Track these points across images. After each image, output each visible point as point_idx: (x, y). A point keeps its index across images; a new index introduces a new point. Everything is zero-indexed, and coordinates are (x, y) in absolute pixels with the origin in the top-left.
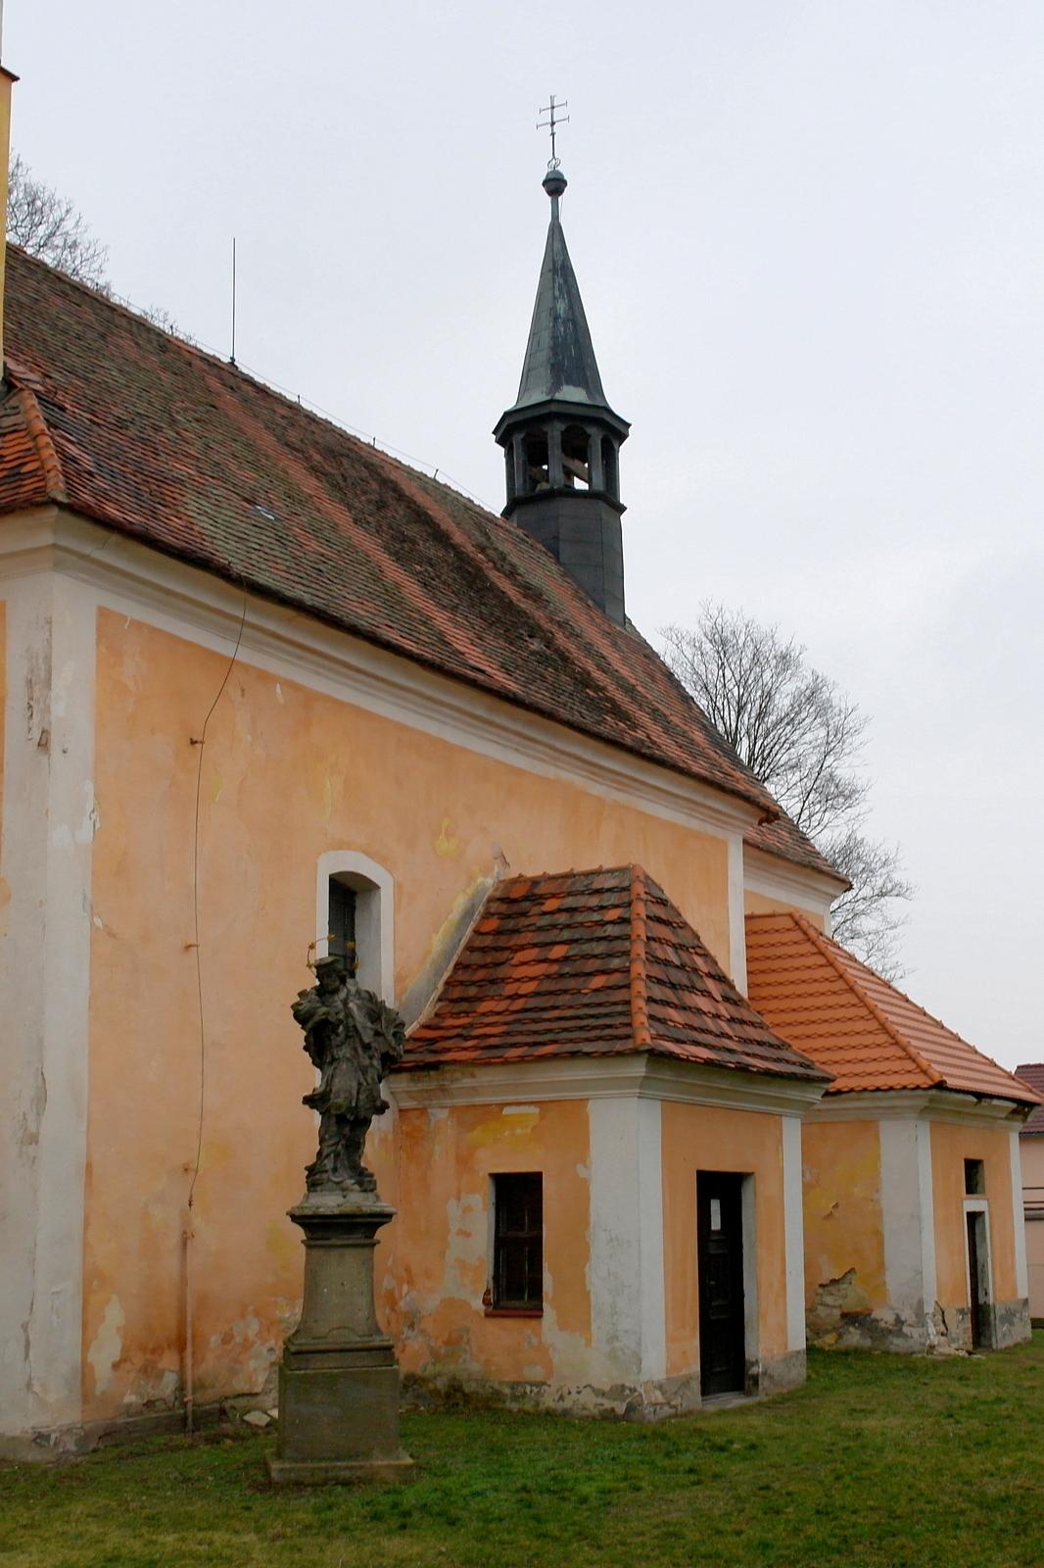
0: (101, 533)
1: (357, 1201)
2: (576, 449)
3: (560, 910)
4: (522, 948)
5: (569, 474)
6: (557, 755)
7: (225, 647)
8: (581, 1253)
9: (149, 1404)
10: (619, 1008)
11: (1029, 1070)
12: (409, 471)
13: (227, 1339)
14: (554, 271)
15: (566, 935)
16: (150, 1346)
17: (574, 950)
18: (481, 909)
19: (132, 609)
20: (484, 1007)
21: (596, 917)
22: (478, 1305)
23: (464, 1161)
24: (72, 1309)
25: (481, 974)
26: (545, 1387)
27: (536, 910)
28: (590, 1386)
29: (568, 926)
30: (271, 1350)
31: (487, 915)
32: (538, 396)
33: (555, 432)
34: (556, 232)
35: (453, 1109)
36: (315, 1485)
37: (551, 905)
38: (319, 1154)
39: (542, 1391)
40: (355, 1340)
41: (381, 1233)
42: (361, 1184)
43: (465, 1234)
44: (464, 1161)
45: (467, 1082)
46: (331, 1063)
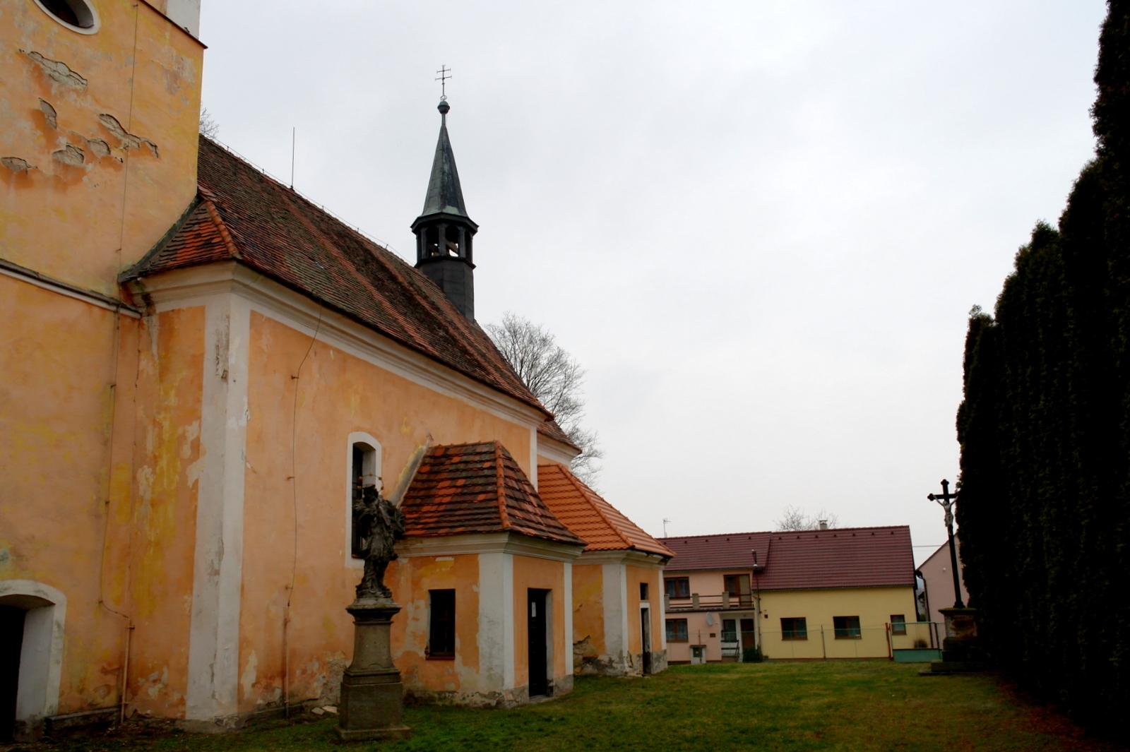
0: (255, 274)
1: (383, 602)
2: (453, 236)
3: (460, 462)
4: (442, 480)
5: (448, 248)
6: (455, 387)
7: (310, 332)
8: (475, 628)
9: (269, 704)
10: (493, 510)
11: (883, 530)
12: (375, 245)
13: (304, 672)
14: (443, 150)
15: (464, 474)
16: (269, 675)
17: (469, 482)
18: (420, 461)
19: (267, 313)
20: (425, 509)
21: (479, 466)
22: (422, 654)
23: (416, 584)
24: (234, 658)
25: (422, 493)
26: (456, 694)
27: (448, 462)
28: (478, 692)
29: (464, 470)
30: (324, 677)
31: (424, 464)
32: (434, 211)
33: (442, 228)
34: (444, 131)
35: (411, 558)
36: (363, 741)
37: (456, 459)
38: (364, 580)
40: (381, 669)
41: (394, 617)
42: (384, 594)
43: (416, 619)
44: (416, 584)
45: (419, 545)
46: (370, 536)
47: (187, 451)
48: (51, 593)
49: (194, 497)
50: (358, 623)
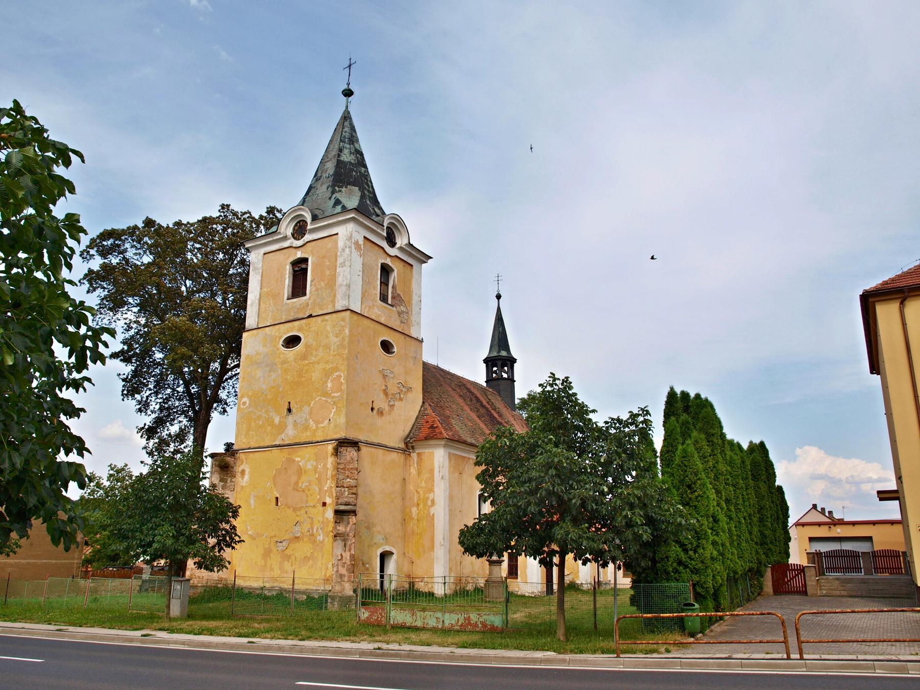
19: (453, 451)
32: (495, 354)
33: (499, 363)
34: (499, 309)
47: (429, 503)
48: (394, 551)
49: (433, 519)
50: (490, 565)
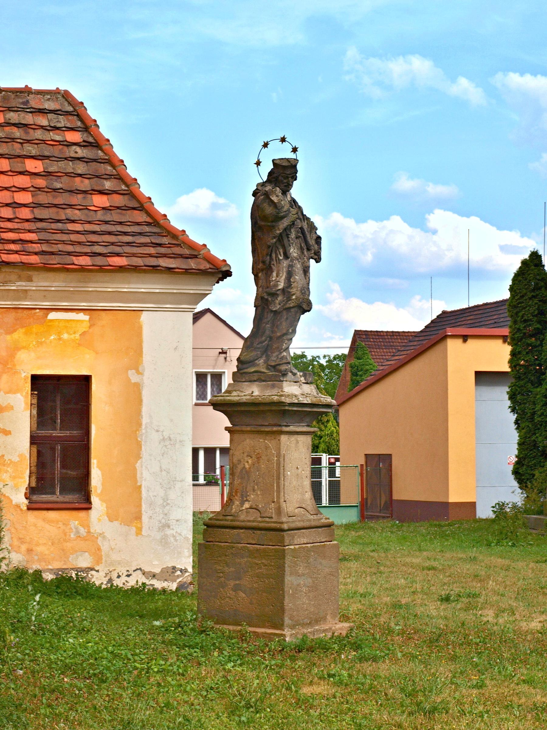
26: (93, 572)
28: (140, 569)
39: (89, 575)
